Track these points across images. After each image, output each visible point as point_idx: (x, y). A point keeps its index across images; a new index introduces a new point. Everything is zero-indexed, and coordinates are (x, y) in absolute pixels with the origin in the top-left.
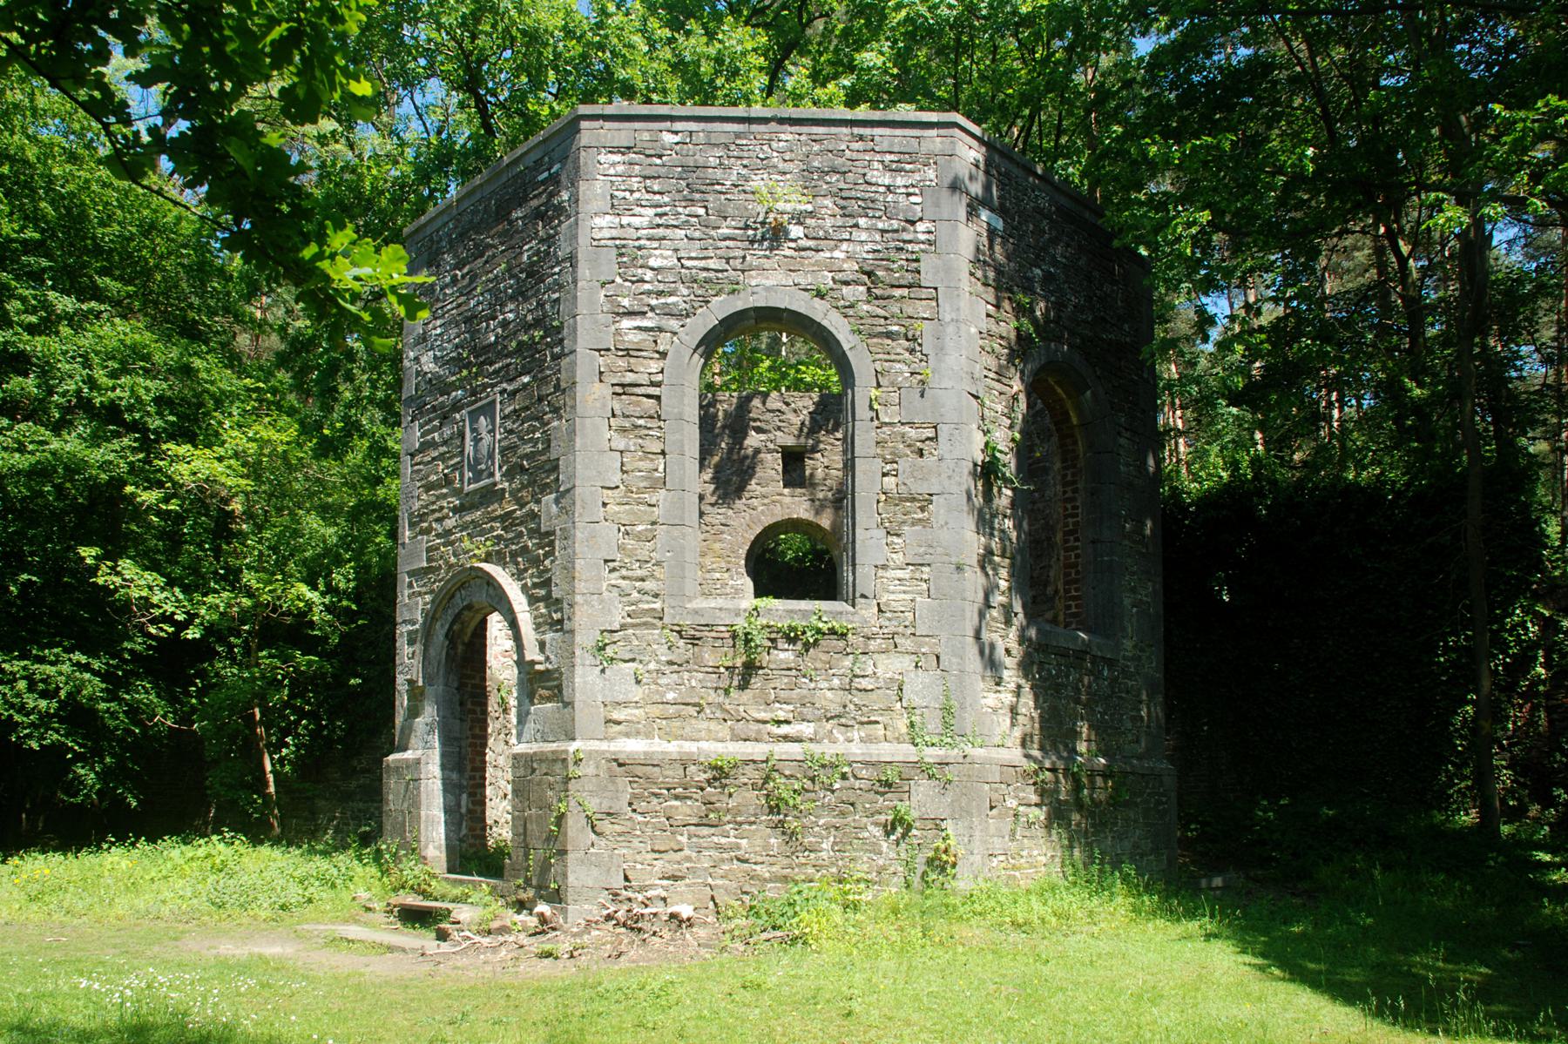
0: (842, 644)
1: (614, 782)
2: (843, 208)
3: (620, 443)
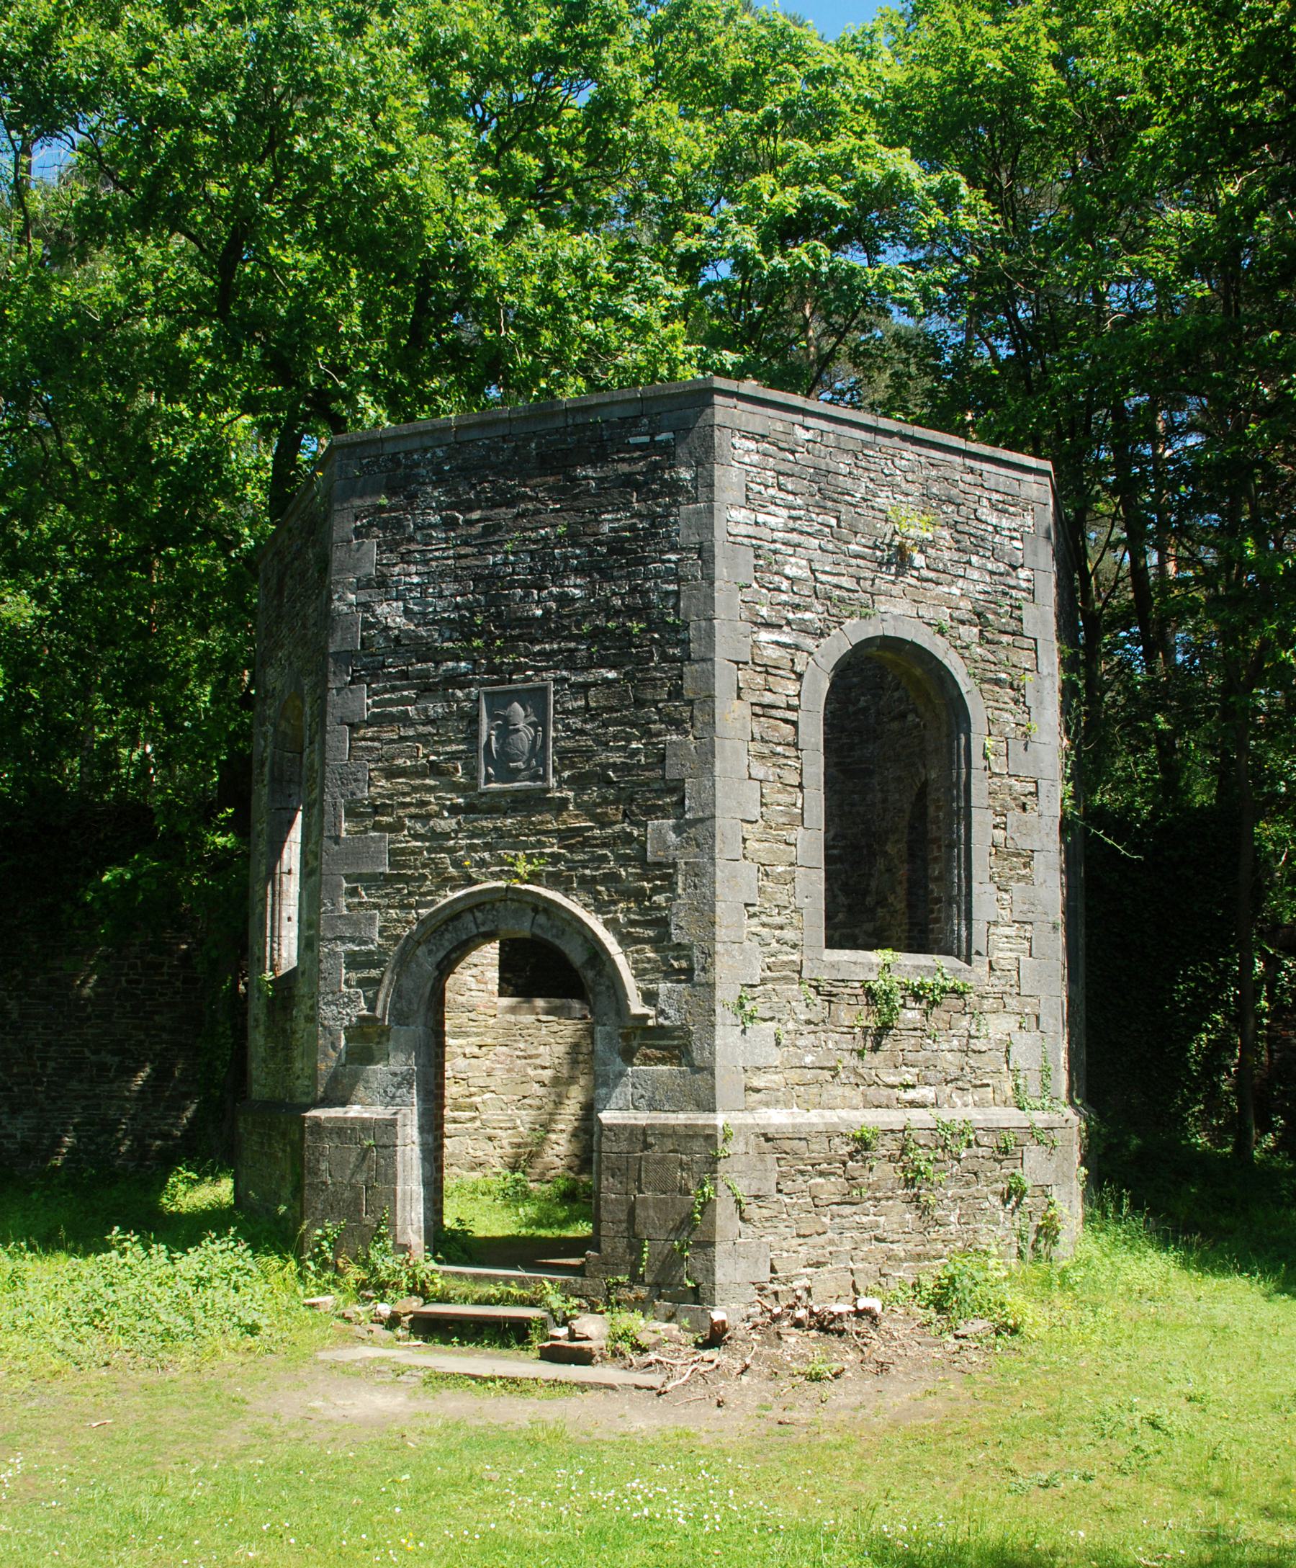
0: (961, 1002)
1: (762, 1160)
2: (958, 542)
3: (759, 771)
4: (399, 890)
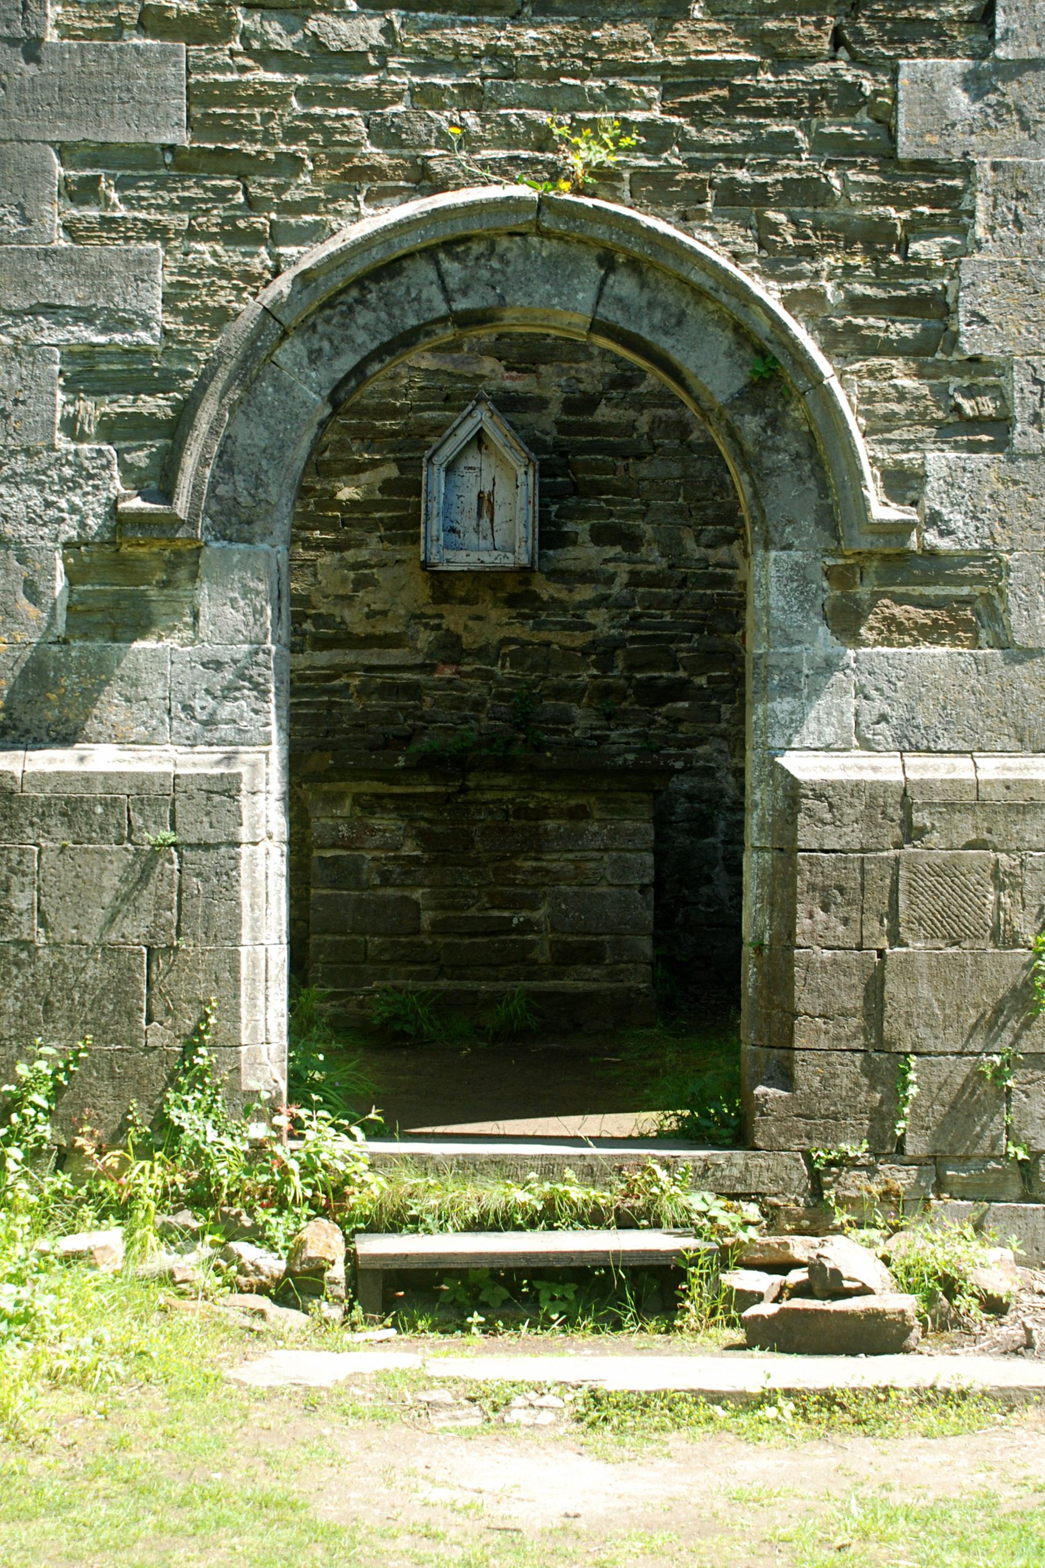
4: (222, 195)
